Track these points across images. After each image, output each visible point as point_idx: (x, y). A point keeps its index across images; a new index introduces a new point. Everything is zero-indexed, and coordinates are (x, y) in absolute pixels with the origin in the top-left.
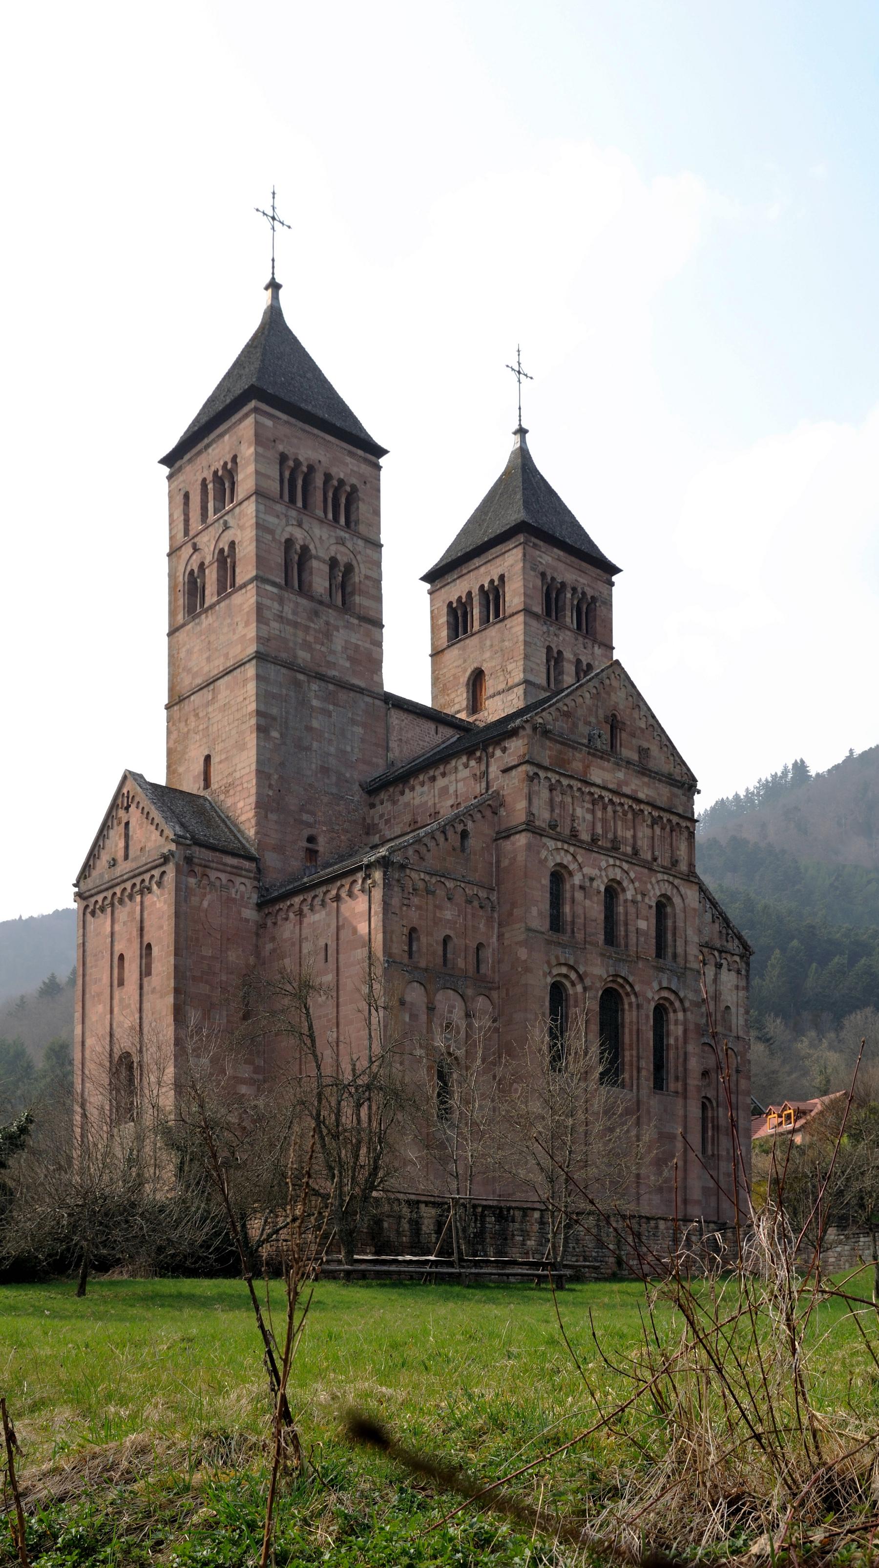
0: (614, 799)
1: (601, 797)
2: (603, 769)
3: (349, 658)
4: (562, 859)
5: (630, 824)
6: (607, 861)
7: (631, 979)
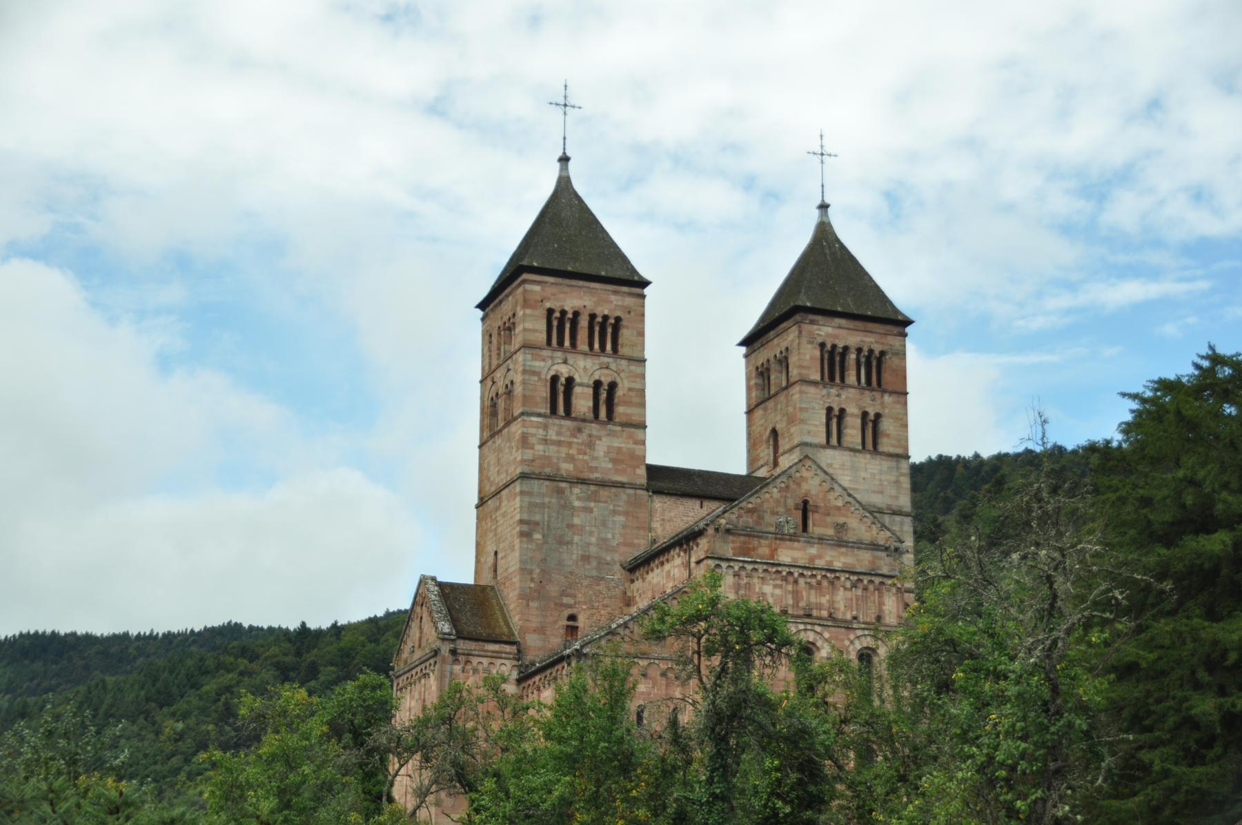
0: (805, 572)
1: (790, 573)
2: (793, 549)
3: (614, 461)
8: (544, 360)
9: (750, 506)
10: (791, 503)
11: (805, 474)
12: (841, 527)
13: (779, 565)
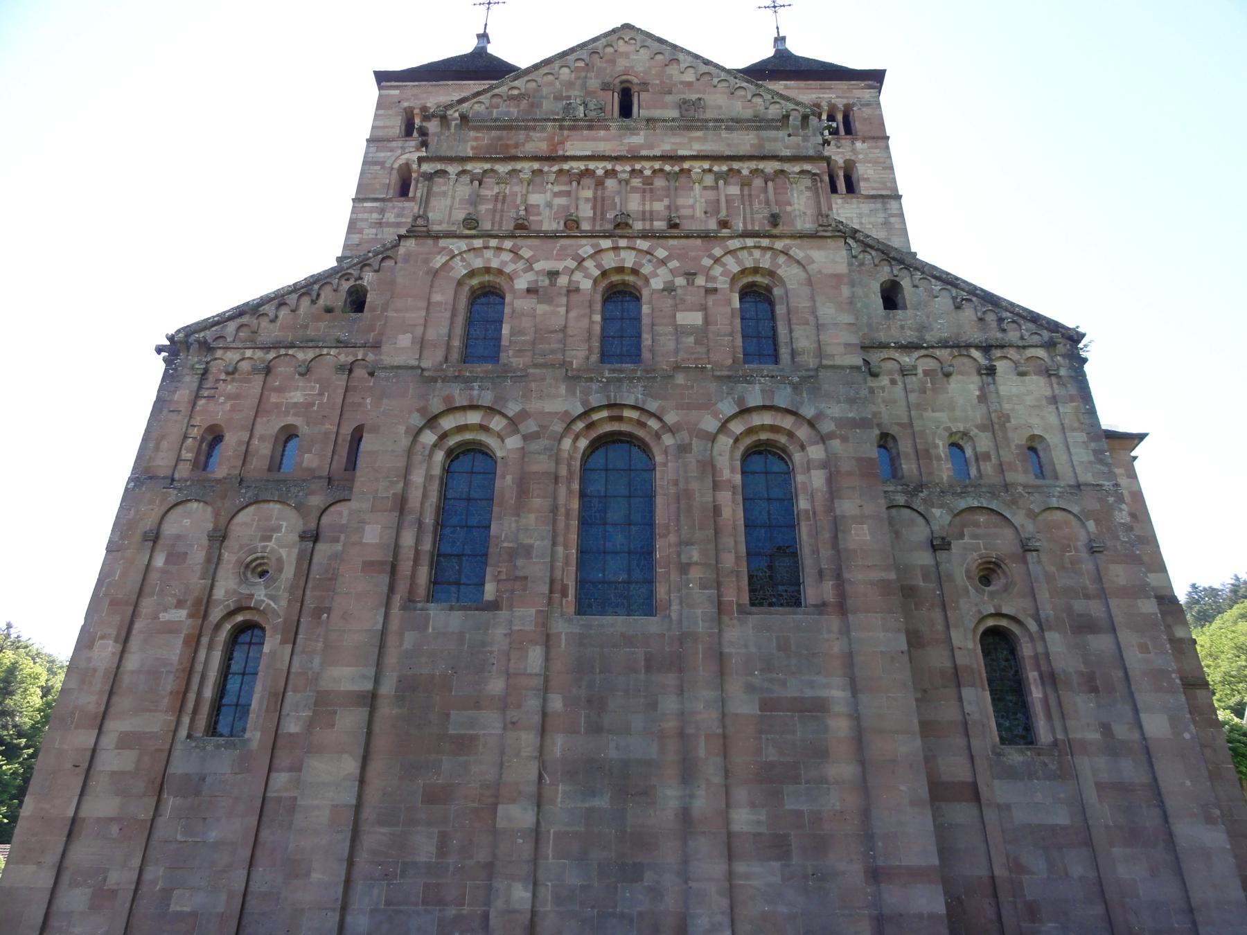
0: (618, 168)
2: (595, 139)
4: (489, 260)
6: (592, 246)
7: (652, 406)
8: (392, 151)
9: (516, 92)
10: (594, 84)
11: (621, 47)
13: (566, 159)
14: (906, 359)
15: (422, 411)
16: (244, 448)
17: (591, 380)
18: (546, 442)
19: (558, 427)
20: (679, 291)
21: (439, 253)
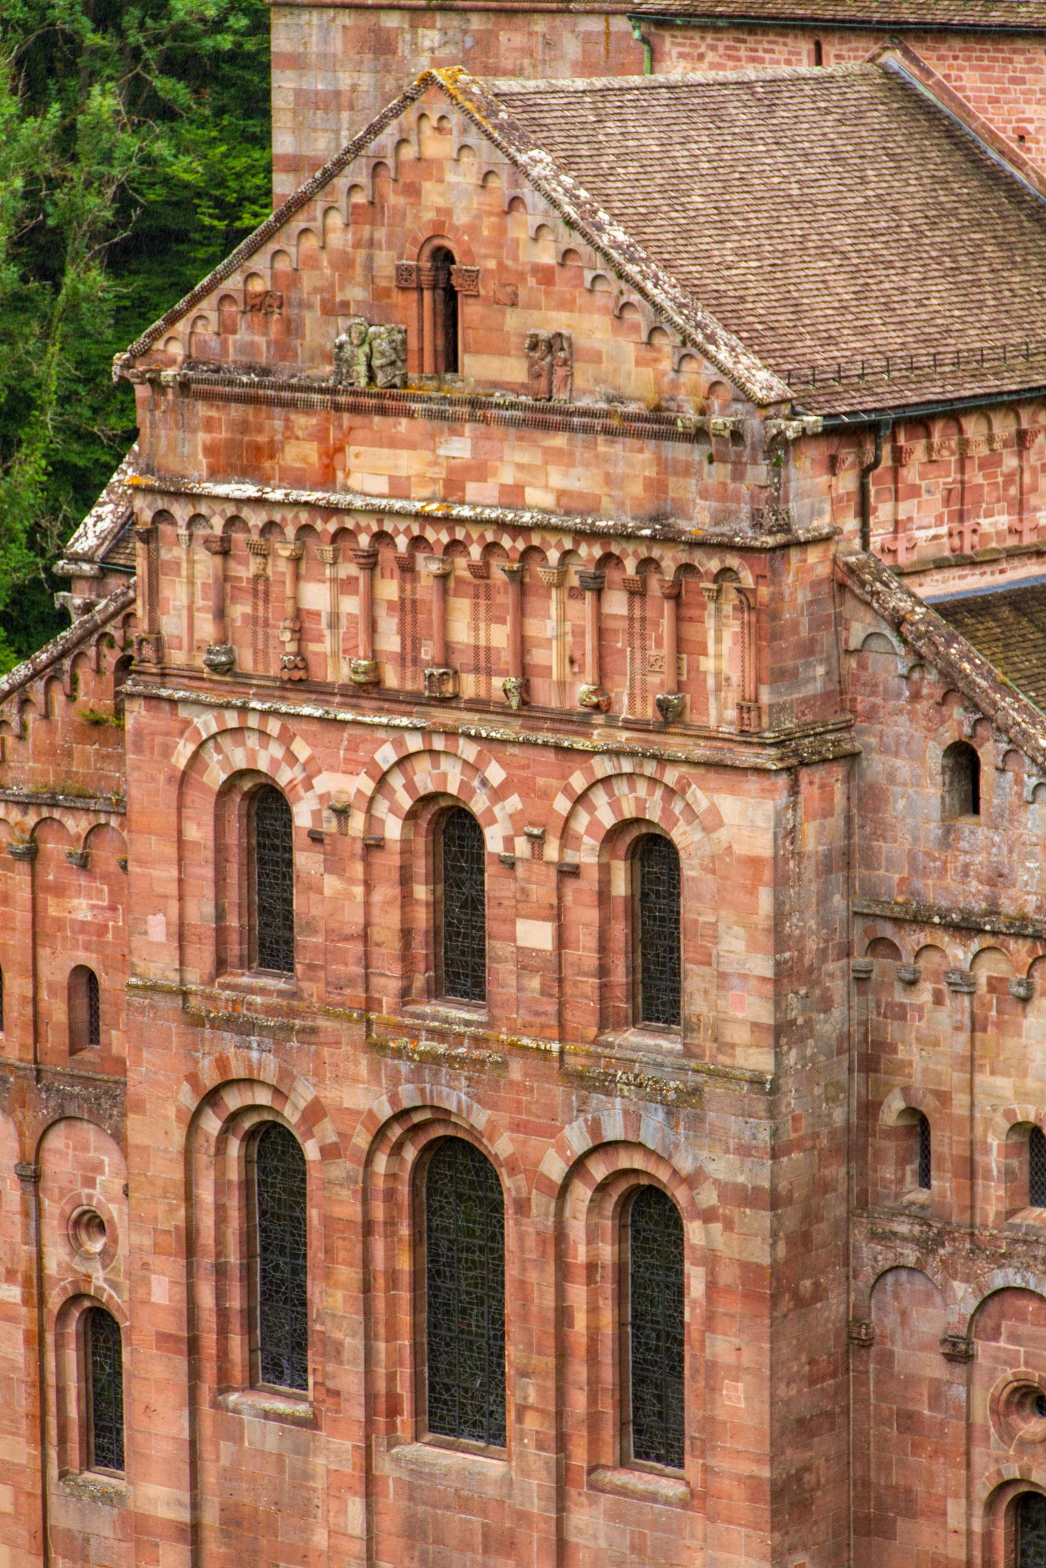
0: (430, 535)
2: (394, 443)
4: (252, 755)
5: (506, 599)
6: (398, 744)
9: (257, 286)
12: (550, 350)
14: (959, 953)
15: (193, 1079)
16: (29, 1010)
17: (398, 1053)
18: (349, 1166)
19: (362, 1140)
20: (520, 870)
21: (181, 734)
